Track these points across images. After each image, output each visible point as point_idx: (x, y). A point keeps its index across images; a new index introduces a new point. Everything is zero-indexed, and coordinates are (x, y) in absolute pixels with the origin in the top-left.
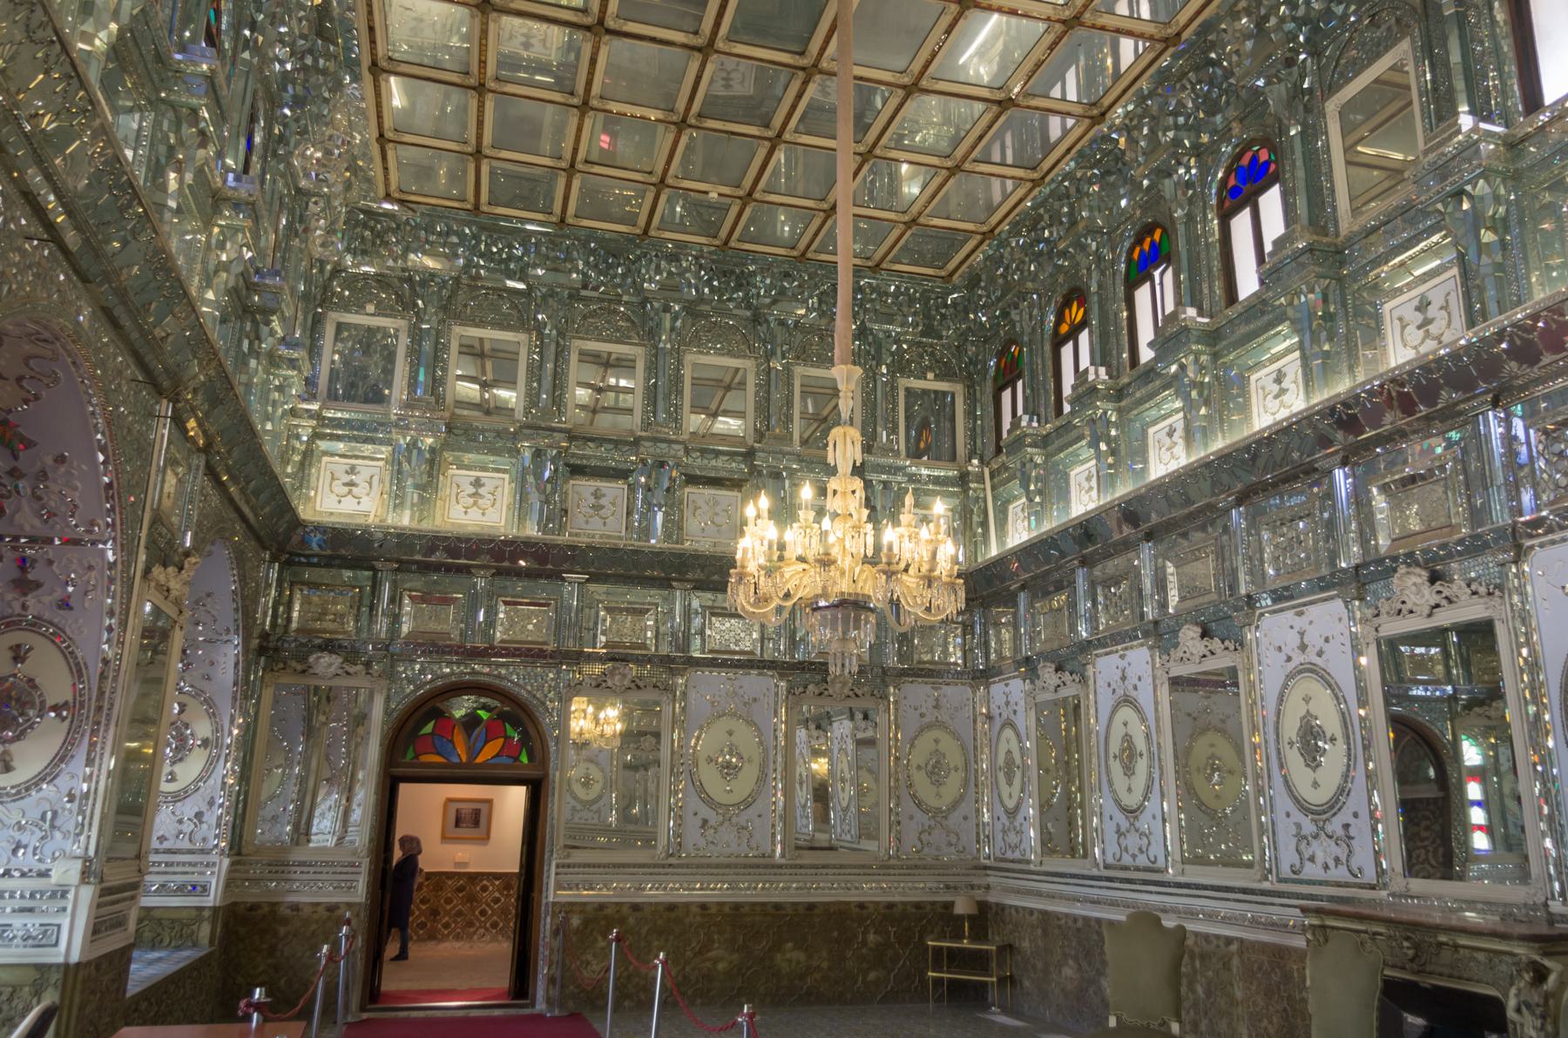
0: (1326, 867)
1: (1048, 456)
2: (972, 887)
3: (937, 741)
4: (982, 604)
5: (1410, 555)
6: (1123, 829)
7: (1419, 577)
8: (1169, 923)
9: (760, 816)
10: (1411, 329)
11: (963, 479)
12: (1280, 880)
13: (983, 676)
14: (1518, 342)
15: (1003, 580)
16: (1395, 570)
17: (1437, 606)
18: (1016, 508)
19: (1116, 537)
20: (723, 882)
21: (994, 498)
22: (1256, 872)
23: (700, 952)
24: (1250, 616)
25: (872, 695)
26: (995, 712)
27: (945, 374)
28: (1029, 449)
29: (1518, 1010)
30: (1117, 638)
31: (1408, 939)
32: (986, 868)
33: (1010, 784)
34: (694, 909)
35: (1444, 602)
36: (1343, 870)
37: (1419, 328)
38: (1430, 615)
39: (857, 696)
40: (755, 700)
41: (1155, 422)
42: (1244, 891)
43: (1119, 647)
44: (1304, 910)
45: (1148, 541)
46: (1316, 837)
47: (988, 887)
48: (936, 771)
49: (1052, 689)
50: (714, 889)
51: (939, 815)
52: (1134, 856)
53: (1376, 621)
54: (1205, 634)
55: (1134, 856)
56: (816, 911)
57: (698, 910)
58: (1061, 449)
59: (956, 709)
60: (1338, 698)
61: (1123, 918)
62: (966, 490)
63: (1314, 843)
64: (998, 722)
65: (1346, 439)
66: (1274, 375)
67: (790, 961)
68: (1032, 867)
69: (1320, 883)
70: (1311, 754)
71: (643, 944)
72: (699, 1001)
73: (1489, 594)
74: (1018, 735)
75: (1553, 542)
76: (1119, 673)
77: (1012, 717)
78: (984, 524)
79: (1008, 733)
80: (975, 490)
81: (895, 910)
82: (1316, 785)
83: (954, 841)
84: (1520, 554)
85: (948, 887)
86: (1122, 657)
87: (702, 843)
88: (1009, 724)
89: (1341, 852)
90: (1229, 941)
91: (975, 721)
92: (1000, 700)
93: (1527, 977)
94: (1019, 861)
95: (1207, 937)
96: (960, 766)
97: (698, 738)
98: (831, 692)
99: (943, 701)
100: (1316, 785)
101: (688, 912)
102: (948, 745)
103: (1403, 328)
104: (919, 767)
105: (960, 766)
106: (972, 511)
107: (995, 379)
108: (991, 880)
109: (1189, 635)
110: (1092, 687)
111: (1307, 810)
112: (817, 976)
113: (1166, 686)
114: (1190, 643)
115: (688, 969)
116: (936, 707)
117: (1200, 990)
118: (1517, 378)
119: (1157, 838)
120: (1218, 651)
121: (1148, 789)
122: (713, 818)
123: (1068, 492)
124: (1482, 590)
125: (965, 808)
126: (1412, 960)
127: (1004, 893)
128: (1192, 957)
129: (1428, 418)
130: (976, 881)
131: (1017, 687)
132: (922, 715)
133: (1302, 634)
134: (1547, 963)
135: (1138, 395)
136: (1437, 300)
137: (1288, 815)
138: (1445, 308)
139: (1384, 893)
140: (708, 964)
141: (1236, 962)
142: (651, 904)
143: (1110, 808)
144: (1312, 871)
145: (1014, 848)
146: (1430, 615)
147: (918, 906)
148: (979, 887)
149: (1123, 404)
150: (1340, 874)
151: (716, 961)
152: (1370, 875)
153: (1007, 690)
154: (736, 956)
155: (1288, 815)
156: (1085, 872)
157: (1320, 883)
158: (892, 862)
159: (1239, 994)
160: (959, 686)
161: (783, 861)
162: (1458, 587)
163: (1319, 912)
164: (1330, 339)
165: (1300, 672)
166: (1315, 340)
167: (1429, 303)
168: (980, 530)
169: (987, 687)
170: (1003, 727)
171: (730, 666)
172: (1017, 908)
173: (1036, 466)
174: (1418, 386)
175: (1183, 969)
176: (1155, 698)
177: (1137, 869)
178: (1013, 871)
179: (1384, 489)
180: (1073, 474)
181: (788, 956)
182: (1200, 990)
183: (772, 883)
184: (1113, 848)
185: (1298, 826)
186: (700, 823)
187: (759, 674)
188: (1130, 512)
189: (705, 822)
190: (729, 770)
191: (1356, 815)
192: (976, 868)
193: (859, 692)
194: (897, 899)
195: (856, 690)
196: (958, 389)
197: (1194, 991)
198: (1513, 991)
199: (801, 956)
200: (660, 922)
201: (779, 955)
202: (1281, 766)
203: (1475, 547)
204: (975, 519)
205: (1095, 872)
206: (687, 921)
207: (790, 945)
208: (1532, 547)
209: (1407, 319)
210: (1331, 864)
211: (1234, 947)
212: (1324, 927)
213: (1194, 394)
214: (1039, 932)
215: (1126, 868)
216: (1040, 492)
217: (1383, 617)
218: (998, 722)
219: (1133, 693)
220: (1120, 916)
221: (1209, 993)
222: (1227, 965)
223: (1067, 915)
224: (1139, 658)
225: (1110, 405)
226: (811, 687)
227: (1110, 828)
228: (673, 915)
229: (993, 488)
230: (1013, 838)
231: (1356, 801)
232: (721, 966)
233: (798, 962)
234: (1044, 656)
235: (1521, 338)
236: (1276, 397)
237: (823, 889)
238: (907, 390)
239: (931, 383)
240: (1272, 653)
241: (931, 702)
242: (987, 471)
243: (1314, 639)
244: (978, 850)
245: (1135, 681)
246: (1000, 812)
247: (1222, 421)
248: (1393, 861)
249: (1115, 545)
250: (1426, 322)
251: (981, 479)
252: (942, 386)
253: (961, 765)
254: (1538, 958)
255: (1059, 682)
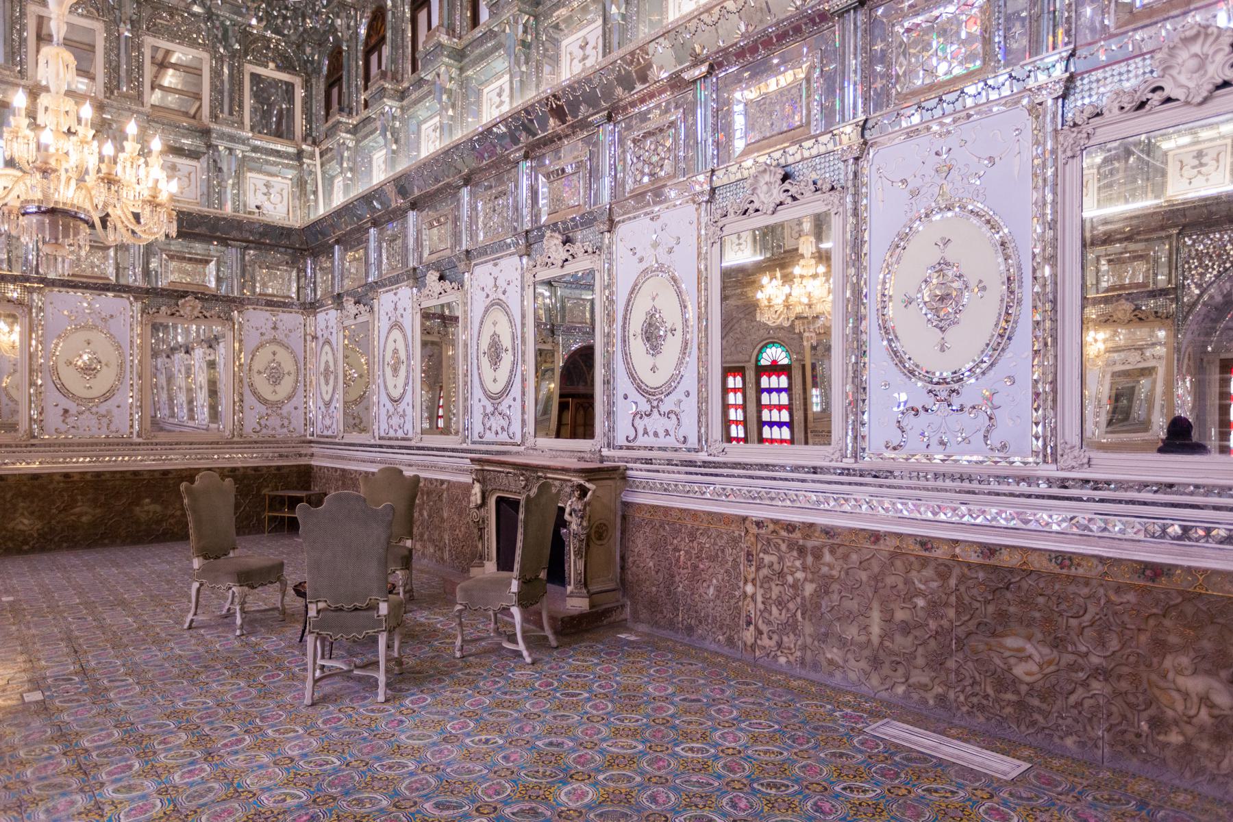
0: (497, 433)
1: (358, 142)
2: (300, 455)
3: (274, 354)
4: (312, 254)
5: (555, 224)
6: (390, 413)
7: (558, 239)
8: (409, 473)
9: (118, 407)
10: (576, 62)
11: (299, 155)
12: (473, 443)
13: (311, 307)
14: (623, 72)
15: (324, 235)
16: (543, 236)
17: (567, 260)
18: (338, 183)
19: (393, 205)
20: (85, 457)
21: (323, 173)
22: (459, 438)
23: (65, 510)
24: (468, 265)
25: (219, 317)
26: (319, 334)
27: (286, 64)
28: (344, 135)
29: (571, 514)
30: (395, 281)
31: (523, 475)
32: (311, 442)
33: (327, 383)
34: (57, 478)
35: (570, 258)
36: (505, 433)
37: (580, 62)
38: (562, 267)
39: (206, 317)
40: (112, 316)
41: (425, 121)
42: (453, 450)
43: (394, 287)
44: (472, 460)
45: (413, 209)
46: (493, 414)
47: (312, 455)
48: (276, 377)
49: (353, 316)
50: (77, 462)
51: (278, 405)
52: (396, 431)
53: (535, 270)
54: (441, 278)
55: (396, 431)
56: (170, 476)
57: (62, 479)
58: (365, 137)
59: (290, 331)
60: (511, 322)
61: (375, 470)
62: (301, 164)
63: (492, 418)
64: (321, 341)
65: (527, 138)
66: (498, 90)
67: (148, 512)
68: (337, 440)
69: (493, 443)
70: (495, 359)
71: (8, 505)
72: (65, 545)
73: (594, 253)
74: (332, 349)
75: (630, 219)
76: (393, 305)
77: (330, 337)
78: (315, 193)
79: (327, 348)
80: (308, 166)
81: (237, 472)
82: (495, 380)
83: (286, 424)
84: (612, 225)
85: (281, 456)
86: (395, 294)
87: (63, 427)
88: (328, 342)
89: (505, 423)
90: (442, 482)
91: (305, 340)
92: (322, 325)
93: (577, 494)
94: (331, 437)
95: (431, 481)
96: (292, 371)
97: (57, 345)
98: (182, 313)
99: (279, 325)
100: (495, 380)
101: (51, 482)
102: (284, 357)
103: (572, 60)
104: (259, 372)
105: (292, 371)
106: (306, 182)
107: (328, 77)
108: (313, 450)
109: (433, 276)
110: (377, 316)
111: (490, 397)
112: (172, 521)
113: (419, 315)
114: (433, 284)
115: (53, 522)
116: (275, 328)
117: (425, 514)
118: (622, 100)
119: (409, 418)
120: (448, 290)
121: (406, 384)
122: (73, 407)
123: (371, 171)
124: (590, 250)
125: (294, 401)
126: (524, 488)
127: (321, 460)
128: (422, 494)
129: (573, 126)
130: (304, 451)
131: (333, 314)
132: (262, 334)
133: (496, 279)
134: (588, 485)
135: (413, 97)
136: (592, 44)
137: (480, 401)
138: (595, 48)
139: (523, 448)
140: (73, 518)
141: (445, 495)
142: (15, 475)
143: (384, 399)
144: (489, 436)
145: (328, 428)
146: (562, 267)
147: (256, 469)
148: (306, 455)
149: (404, 103)
150: (503, 437)
151: (80, 515)
152: (518, 439)
153: (327, 317)
154: (98, 511)
155: (480, 401)
156: (368, 442)
157: (493, 443)
158: (236, 439)
159: (445, 515)
160: (294, 314)
161: (140, 440)
162: (577, 248)
163: (479, 461)
164: (527, 63)
165: (492, 305)
166: (518, 63)
167: (587, 44)
168: (312, 197)
169: (315, 316)
170: (324, 344)
171: (96, 289)
172: (321, 468)
173: (348, 148)
174: (568, 102)
175: (417, 501)
176: (412, 324)
177: (397, 439)
178: (324, 443)
179: (547, 176)
180: (375, 157)
181: (146, 508)
182: (425, 514)
183: (130, 456)
184: (384, 426)
185: (484, 407)
186: (62, 412)
187: (114, 296)
188: (401, 184)
189: (66, 411)
190: (88, 370)
191: (514, 400)
192: (304, 442)
193: (208, 315)
194: (239, 465)
195: (205, 313)
196: (297, 81)
197: (422, 515)
198: (569, 503)
199: (158, 508)
200: (24, 489)
201: (138, 508)
202: (479, 369)
203: (587, 221)
204: (309, 187)
205: (373, 442)
206: (51, 487)
207: (147, 500)
208: (619, 222)
209: (575, 54)
210: (500, 431)
211: (445, 486)
212: (483, 470)
213: (445, 97)
214: (340, 483)
215: (390, 439)
216: (351, 170)
217: (538, 267)
218: (321, 341)
219: (400, 320)
220: (374, 469)
221: (430, 516)
222: (440, 497)
223: (356, 471)
224: (405, 294)
225: (397, 104)
226: (163, 308)
227: (383, 412)
228: (36, 483)
229: (322, 165)
230: (328, 422)
231: (516, 390)
232: (84, 519)
233: (155, 512)
234: (348, 293)
235: (625, 69)
236: (497, 107)
237: (171, 459)
238: (252, 74)
239: (270, 72)
240: (479, 292)
241: (270, 325)
242: (317, 150)
243: (502, 283)
244: (305, 430)
245: (402, 311)
246: (321, 404)
247: (462, 123)
248: (531, 428)
249: (394, 211)
250: (585, 58)
251: (312, 156)
252: (285, 77)
253: (293, 369)
254: (582, 482)
255: (357, 312)
